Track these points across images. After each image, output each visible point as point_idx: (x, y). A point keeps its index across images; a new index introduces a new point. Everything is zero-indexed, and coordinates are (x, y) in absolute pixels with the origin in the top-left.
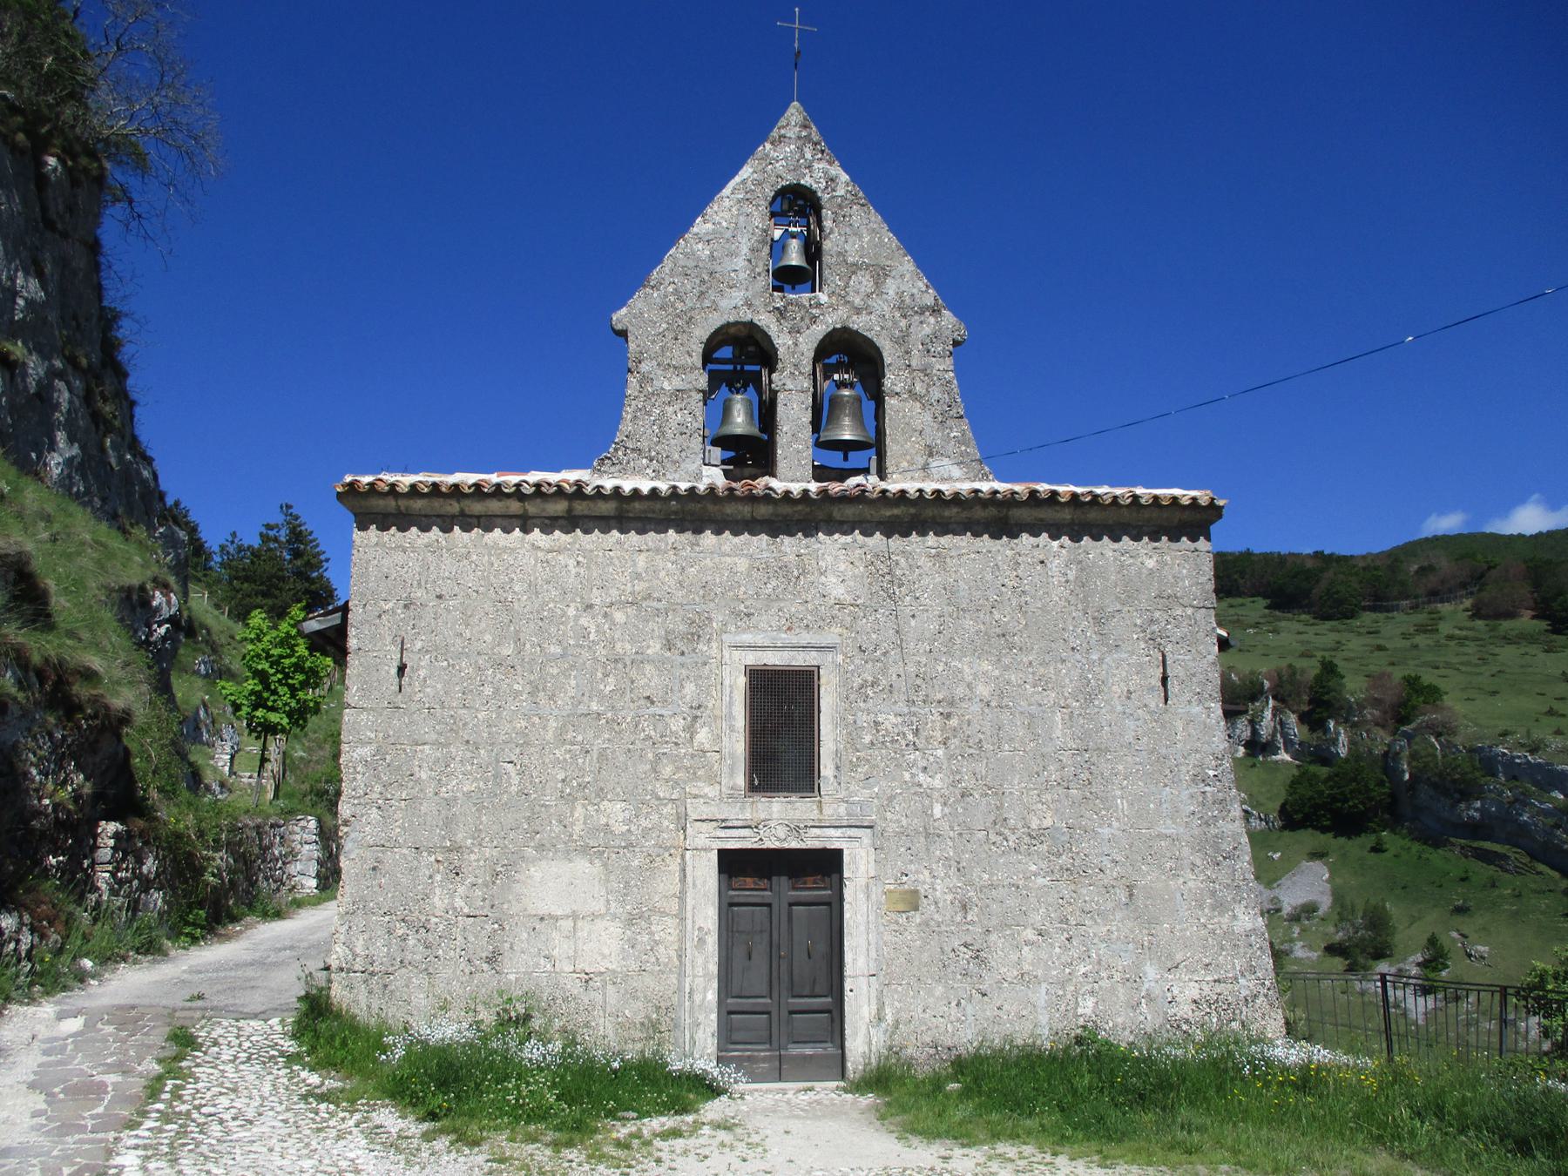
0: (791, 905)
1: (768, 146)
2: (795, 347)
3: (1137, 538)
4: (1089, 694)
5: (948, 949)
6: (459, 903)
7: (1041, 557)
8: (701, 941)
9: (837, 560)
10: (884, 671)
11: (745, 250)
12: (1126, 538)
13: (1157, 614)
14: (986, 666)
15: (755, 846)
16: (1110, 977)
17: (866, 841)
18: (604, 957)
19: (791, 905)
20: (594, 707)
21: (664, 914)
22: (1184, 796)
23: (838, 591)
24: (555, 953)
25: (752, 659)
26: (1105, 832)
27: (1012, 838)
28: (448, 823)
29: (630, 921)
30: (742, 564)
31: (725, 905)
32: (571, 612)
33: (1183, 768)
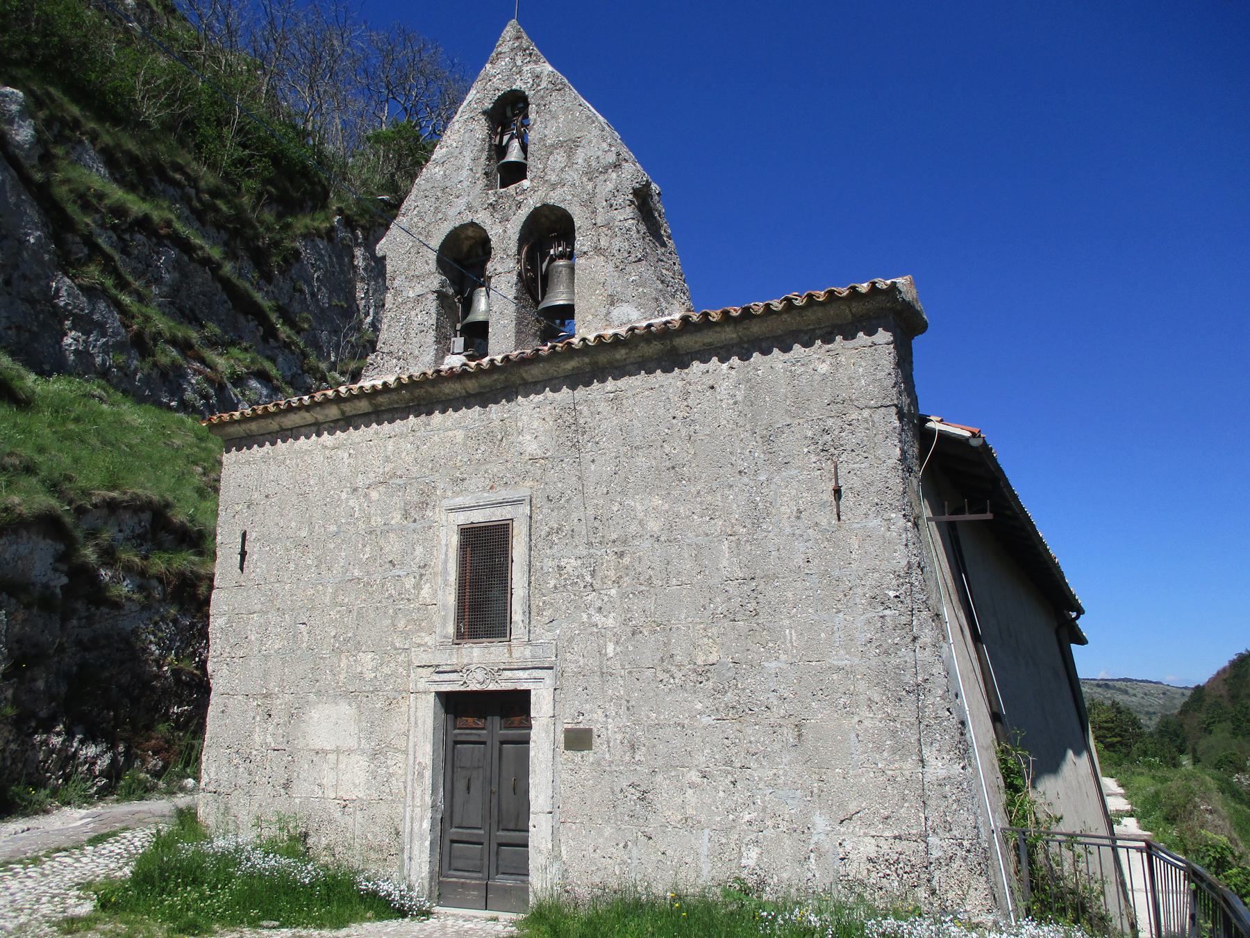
0: (502, 743)
1: (488, 66)
2: (504, 235)
3: (808, 344)
4: (757, 517)
5: (617, 790)
6: (269, 739)
7: (711, 383)
8: (421, 775)
9: (531, 418)
10: (567, 517)
11: (468, 161)
12: (797, 347)
13: (830, 422)
14: (657, 501)
15: (462, 689)
16: (776, 827)
17: (548, 681)
18: (355, 786)
19: (502, 743)
20: (357, 573)
21: (397, 750)
22: (859, 622)
23: (532, 448)
24: (324, 782)
25: (463, 518)
26: (772, 665)
27: (678, 675)
28: (266, 675)
29: (374, 756)
30: (460, 435)
31: (450, 744)
32: (344, 496)
33: (859, 591)
